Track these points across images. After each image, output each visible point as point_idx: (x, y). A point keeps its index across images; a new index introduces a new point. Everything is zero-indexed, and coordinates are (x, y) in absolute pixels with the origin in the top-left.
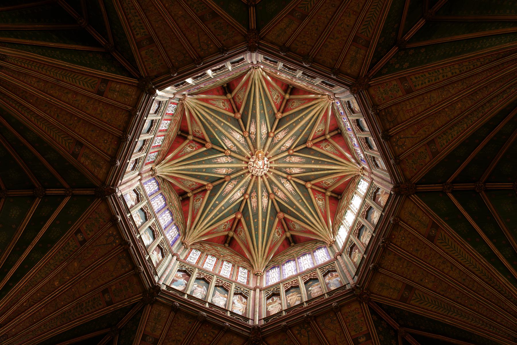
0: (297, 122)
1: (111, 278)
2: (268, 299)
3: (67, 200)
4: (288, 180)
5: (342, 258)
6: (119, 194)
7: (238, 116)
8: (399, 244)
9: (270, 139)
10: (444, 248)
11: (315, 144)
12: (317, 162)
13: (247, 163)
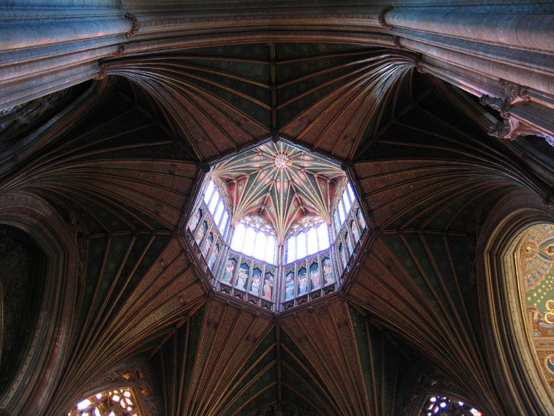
0: (311, 189)
3: (269, 108)
12: (285, 201)
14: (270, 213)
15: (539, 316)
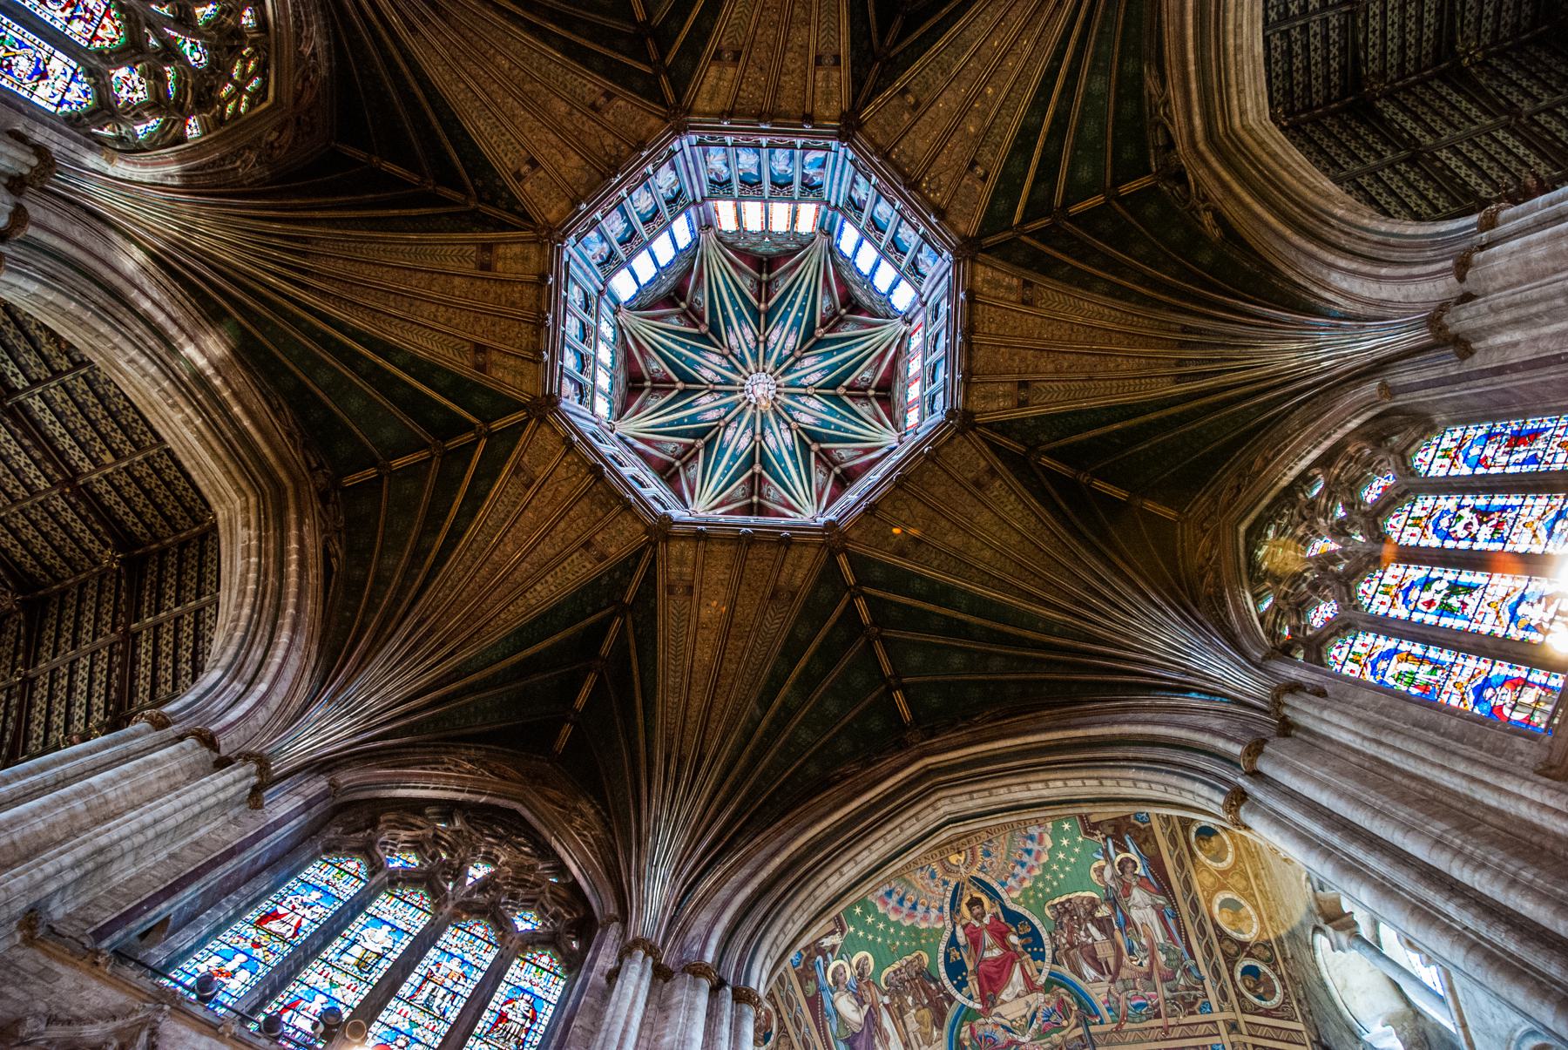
0: (728, 468)
1: (914, 128)
2: (680, 191)
3: (1016, 220)
4: (711, 382)
5: (596, 287)
6: (946, 254)
7: (815, 447)
8: (523, 325)
9: (758, 430)
10: (457, 341)
11: (692, 446)
12: (680, 422)
13: (778, 386)
14: (644, 401)
15: (833, 948)
